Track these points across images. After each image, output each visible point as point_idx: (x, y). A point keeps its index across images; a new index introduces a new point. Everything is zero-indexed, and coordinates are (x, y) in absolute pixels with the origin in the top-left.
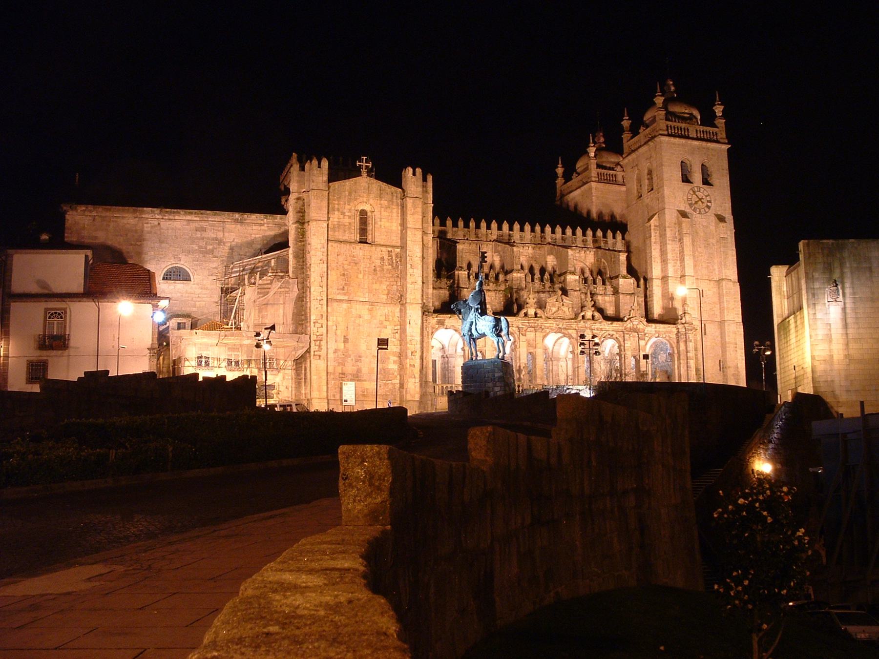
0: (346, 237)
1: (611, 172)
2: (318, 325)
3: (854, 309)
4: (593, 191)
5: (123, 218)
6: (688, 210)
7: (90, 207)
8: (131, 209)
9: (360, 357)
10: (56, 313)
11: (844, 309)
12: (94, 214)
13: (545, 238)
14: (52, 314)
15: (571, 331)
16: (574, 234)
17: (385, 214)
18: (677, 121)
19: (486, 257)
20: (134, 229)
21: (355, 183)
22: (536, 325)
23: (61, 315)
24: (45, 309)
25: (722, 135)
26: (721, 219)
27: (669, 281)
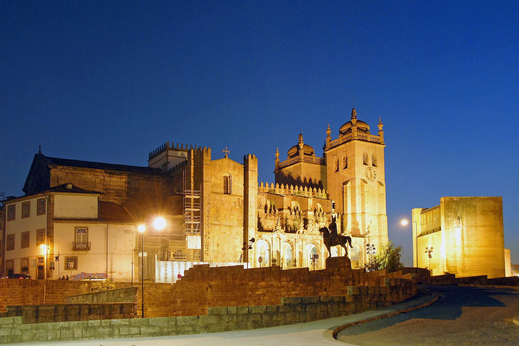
0: (218, 191)
1: (311, 157)
2: (207, 237)
3: (467, 231)
4: (302, 167)
5: (84, 174)
6: (366, 179)
7: (66, 167)
8: (89, 169)
9: (224, 254)
10: (81, 230)
11: (462, 231)
12: (67, 171)
13: (290, 192)
14: (79, 230)
15: (318, 240)
16: (303, 190)
17: (236, 179)
18: (360, 132)
19: (335, 206)
20: (91, 181)
21: (222, 162)
22: (303, 238)
23: (85, 231)
24: (75, 227)
25: (382, 140)
26: (381, 184)
27: (357, 215)
